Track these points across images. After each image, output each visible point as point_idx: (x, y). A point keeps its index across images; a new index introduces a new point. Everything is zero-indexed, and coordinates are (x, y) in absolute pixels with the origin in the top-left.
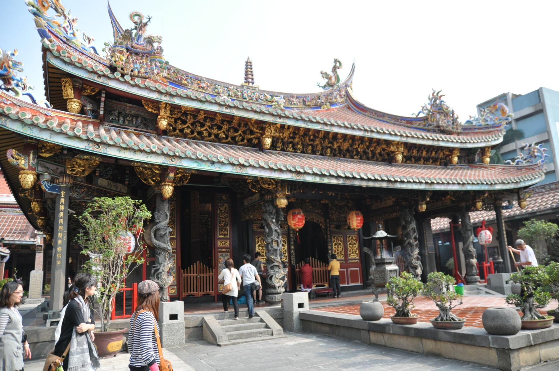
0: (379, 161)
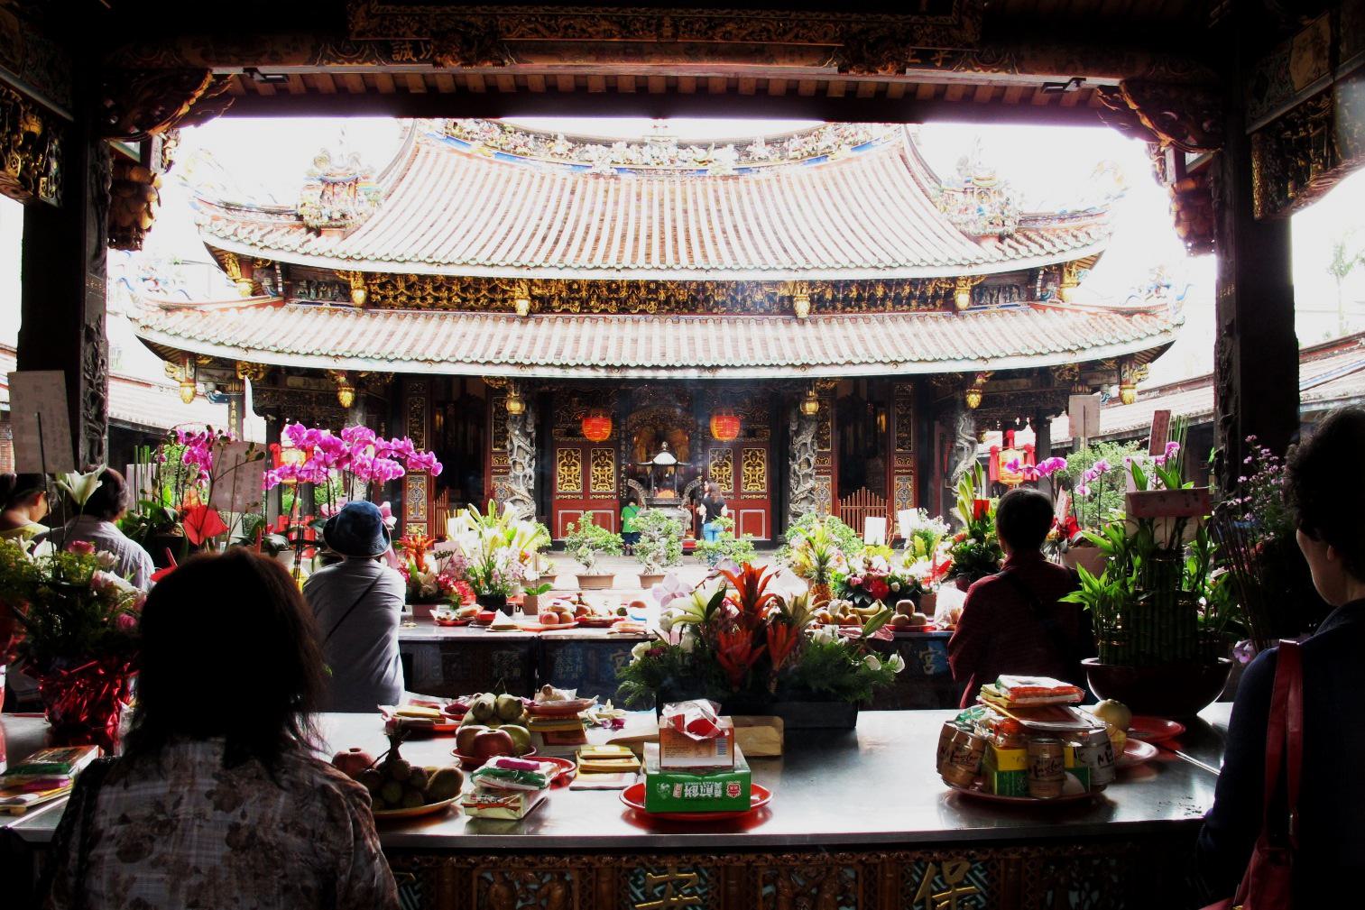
0: (774, 314)
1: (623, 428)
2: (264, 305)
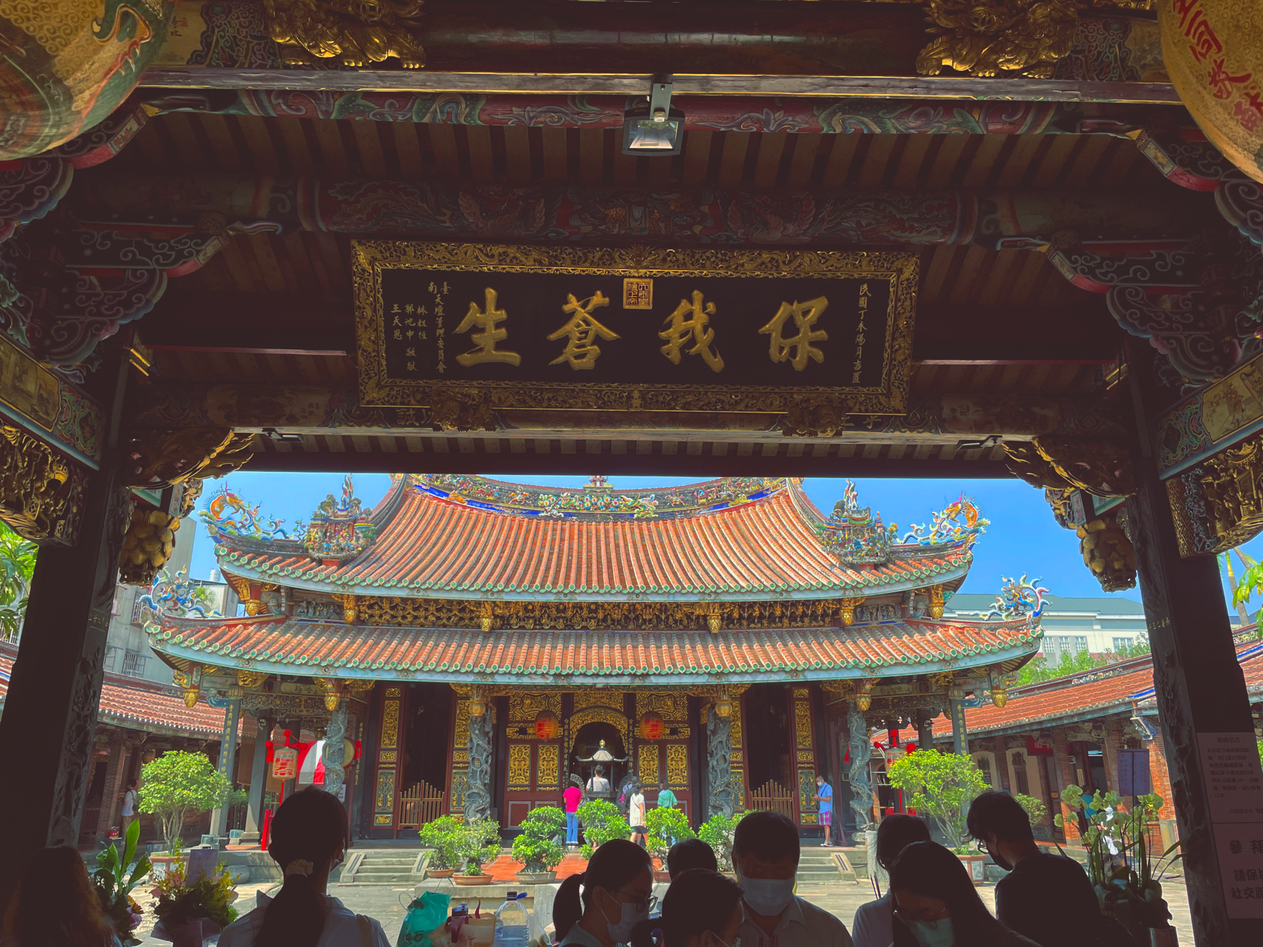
1: (566, 727)
2: (268, 623)
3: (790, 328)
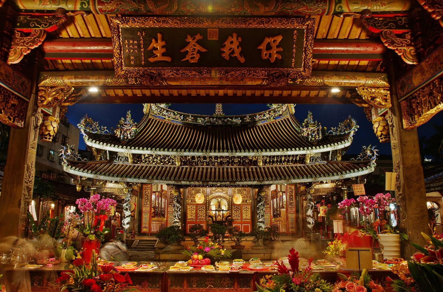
3: (269, 47)
